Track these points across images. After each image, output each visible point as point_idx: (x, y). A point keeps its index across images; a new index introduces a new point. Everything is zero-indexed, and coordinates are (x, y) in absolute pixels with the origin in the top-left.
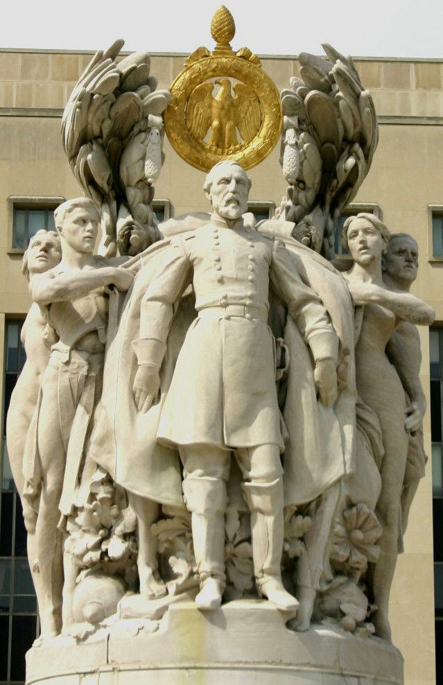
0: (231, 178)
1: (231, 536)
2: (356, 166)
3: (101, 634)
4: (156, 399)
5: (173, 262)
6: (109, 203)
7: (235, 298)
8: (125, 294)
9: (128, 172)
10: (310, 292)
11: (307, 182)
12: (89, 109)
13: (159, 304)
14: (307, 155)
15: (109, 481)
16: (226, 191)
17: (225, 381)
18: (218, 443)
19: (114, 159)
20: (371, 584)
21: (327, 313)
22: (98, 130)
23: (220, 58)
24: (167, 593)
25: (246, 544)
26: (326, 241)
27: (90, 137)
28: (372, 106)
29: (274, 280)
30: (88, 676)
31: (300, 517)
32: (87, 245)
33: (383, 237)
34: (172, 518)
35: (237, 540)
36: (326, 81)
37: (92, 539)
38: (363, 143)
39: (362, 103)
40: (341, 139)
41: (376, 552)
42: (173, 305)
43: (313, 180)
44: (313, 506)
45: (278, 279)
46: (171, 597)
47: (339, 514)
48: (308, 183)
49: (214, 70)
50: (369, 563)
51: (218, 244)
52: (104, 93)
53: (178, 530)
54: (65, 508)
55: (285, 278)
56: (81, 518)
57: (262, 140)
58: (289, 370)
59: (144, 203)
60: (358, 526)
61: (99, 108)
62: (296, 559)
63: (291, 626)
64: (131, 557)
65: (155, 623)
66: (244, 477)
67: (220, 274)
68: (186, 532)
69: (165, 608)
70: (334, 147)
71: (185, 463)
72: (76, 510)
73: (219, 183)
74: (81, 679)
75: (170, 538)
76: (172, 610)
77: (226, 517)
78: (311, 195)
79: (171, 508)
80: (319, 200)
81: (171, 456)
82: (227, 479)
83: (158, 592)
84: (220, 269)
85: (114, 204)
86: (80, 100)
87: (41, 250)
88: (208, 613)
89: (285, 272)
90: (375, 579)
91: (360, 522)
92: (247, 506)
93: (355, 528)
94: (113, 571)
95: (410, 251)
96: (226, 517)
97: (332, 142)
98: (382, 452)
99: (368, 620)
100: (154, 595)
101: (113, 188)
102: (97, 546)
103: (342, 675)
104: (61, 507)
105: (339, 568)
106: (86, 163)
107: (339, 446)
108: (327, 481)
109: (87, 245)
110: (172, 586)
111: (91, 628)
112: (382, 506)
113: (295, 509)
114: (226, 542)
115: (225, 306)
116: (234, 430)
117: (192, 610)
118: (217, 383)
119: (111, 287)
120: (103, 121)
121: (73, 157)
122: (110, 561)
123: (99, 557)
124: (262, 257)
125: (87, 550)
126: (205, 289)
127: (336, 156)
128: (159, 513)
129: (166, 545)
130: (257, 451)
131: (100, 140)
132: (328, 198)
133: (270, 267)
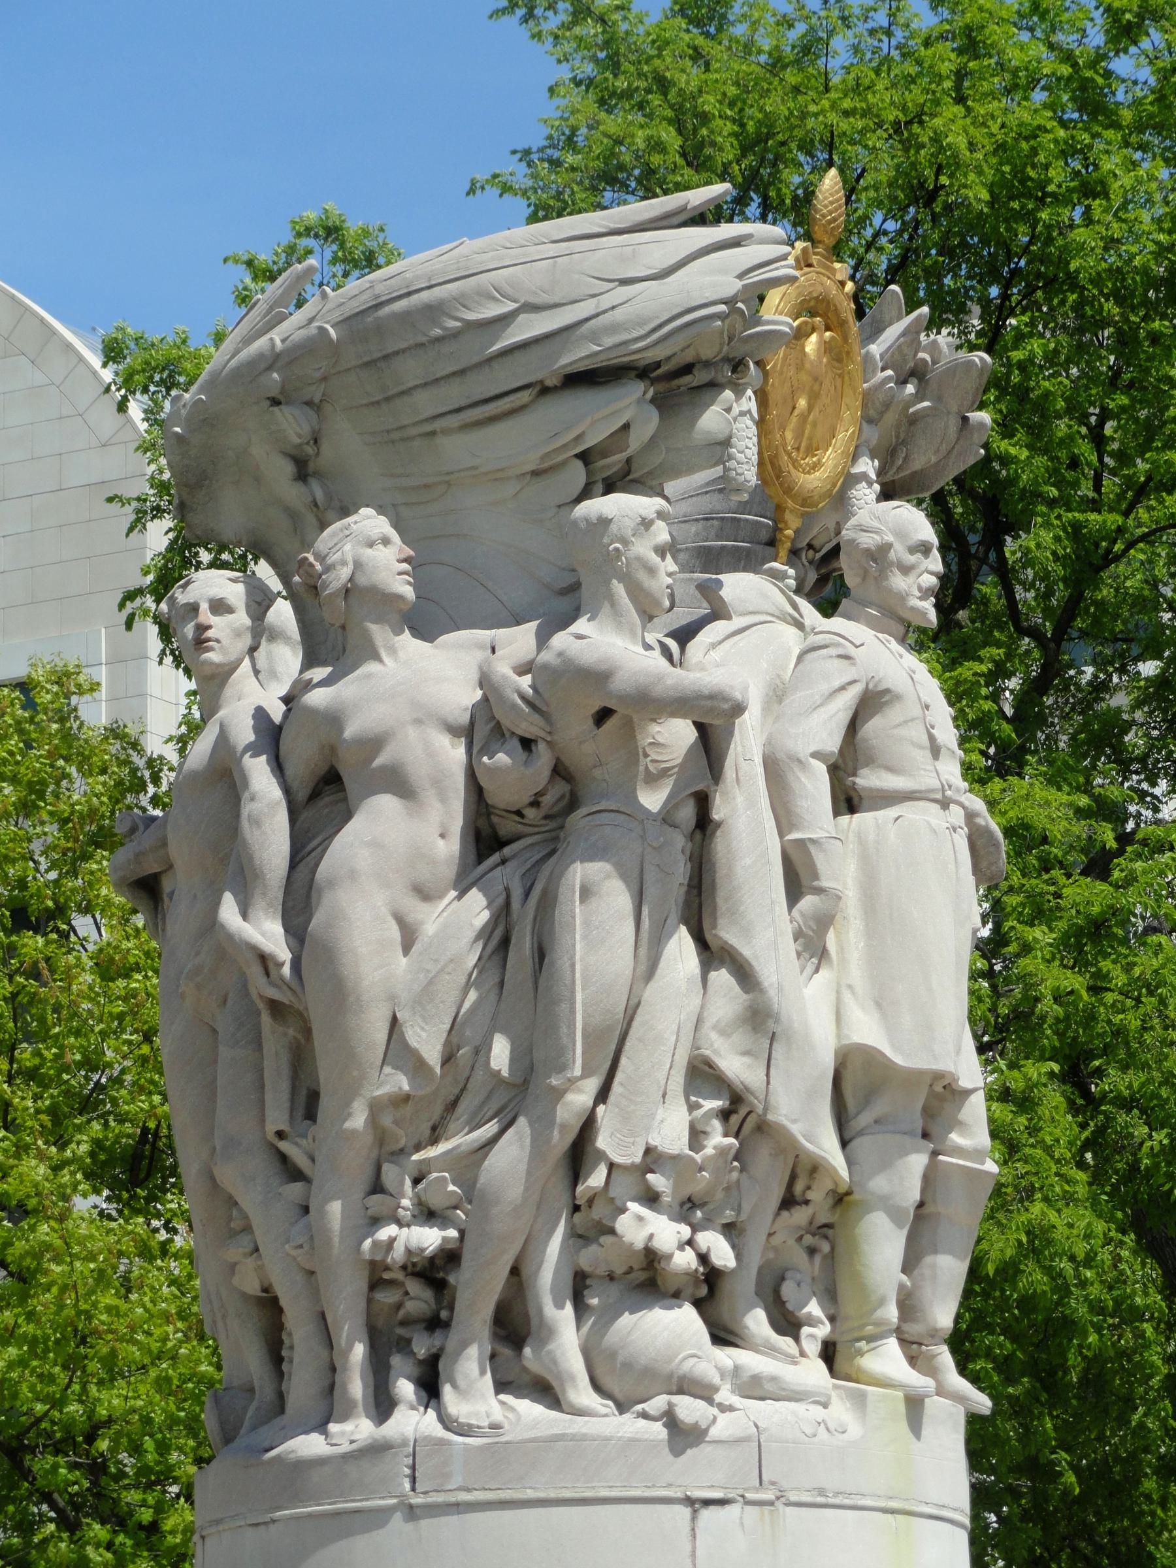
5: (843, 688)
30: (712, 1508)
34: (807, 1202)
72: (652, 1158)
73: (912, 550)
74: (695, 1511)
81: (856, 1088)
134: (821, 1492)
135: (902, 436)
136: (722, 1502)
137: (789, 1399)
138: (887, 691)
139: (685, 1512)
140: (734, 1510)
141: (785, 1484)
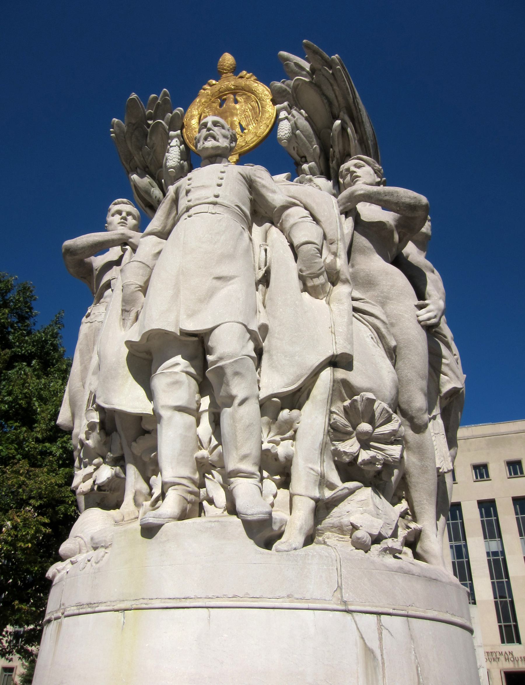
55: (264, 191)
89: (264, 186)
116: (192, 315)
130: (216, 331)
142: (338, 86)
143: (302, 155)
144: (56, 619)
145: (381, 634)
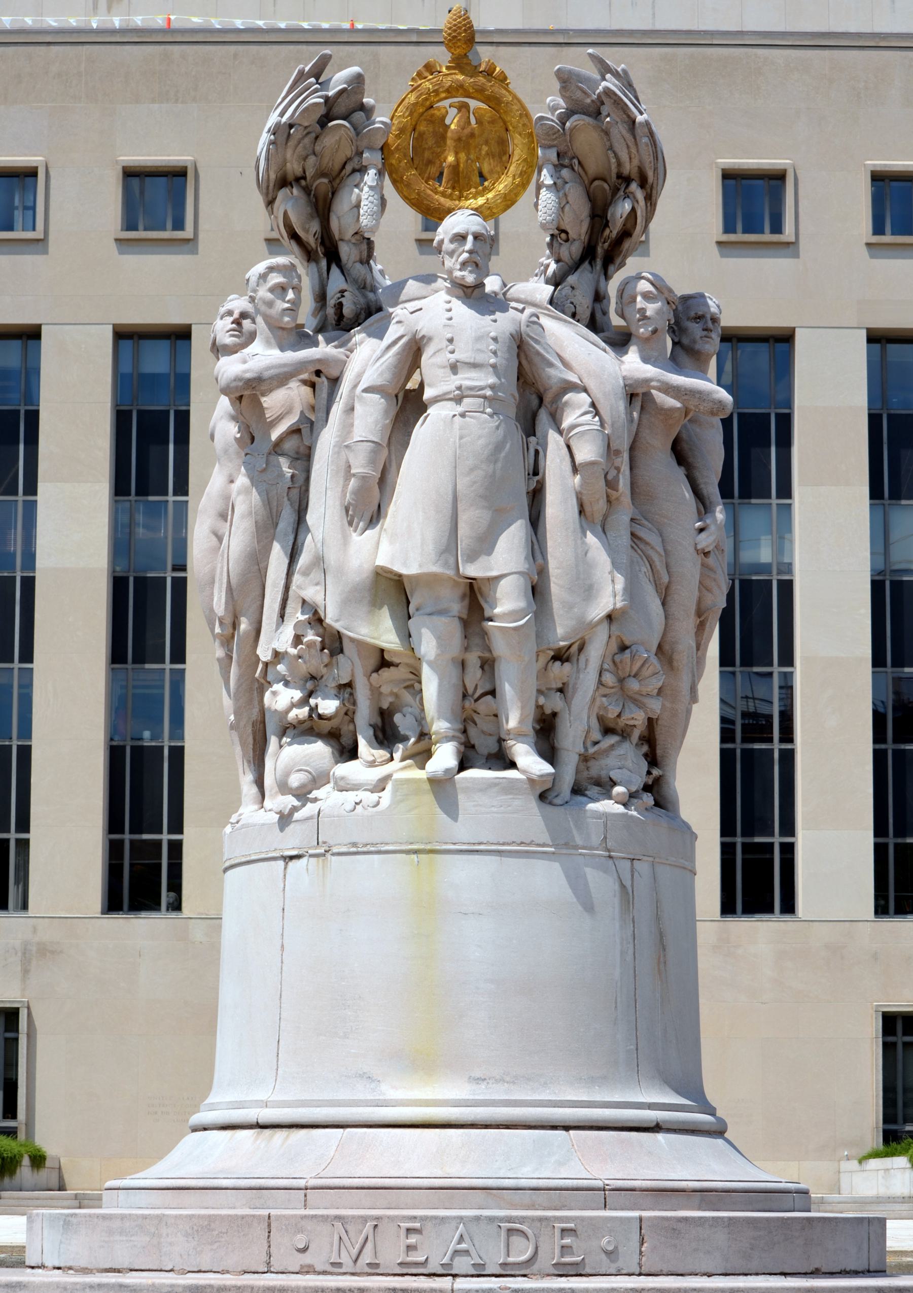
0: (467, 234)
1: (470, 691)
2: (633, 210)
3: (309, 809)
4: (375, 516)
6: (317, 261)
7: (471, 388)
8: (335, 382)
9: (339, 223)
10: (573, 378)
11: (569, 231)
12: (286, 143)
13: (376, 397)
14: (569, 198)
15: (317, 620)
16: (461, 249)
17: (459, 494)
18: (451, 573)
19: (322, 207)
20: (653, 748)
21: (593, 405)
22: (301, 169)
23: (455, 74)
24: (392, 759)
25: (489, 697)
26: (597, 306)
27: (290, 177)
28: (651, 134)
29: (524, 362)
31: (558, 663)
32: (286, 319)
33: (668, 303)
34: (397, 665)
35: (479, 692)
36: (593, 101)
37: (297, 695)
38: (643, 182)
39: (639, 131)
40: (614, 176)
41: (655, 706)
42: (396, 396)
43: (579, 229)
44: (575, 648)
45: (530, 362)
46: (396, 764)
47: (609, 660)
48: (572, 234)
49: (448, 91)
50: (650, 720)
51: (450, 319)
52: (306, 124)
53: (405, 680)
54: (264, 653)
55: (536, 360)
56: (281, 668)
57: (510, 179)
58: (544, 478)
59: (361, 262)
60: (633, 674)
61: (299, 143)
62: (554, 714)
63: (546, 798)
64: (348, 713)
65: (374, 797)
66: (487, 614)
67: (453, 358)
68: (414, 685)
69: (388, 778)
70: (606, 186)
71: (412, 596)
72: (278, 656)
75: (395, 690)
76: (396, 780)
77: (463, 664)
78: (576, 249)
79: (395, 653)
80: (588, 254)
81: (393, 591)
82: (465, 616)
83: (381, 757)
84: (452, 352)
85: (324, 263)
86: (274, 134)
87: (233, 323)
88: (440, 786)
90: (657, 737)
91: (635, 668)
92: (490, 651)
93: (629, 676)
94: (326, 731)
95: (708, 317)
96: (463, 664)
97: (605, 180)
98: (665, 579)
99: (647, 788)
100: (374, 761)
101: (323, 243)
102: (304, 701)
103: (610, 857)
104: (259, 652)
105: (612, 725)
106: (285, 213)
107: (607, 574)
108: (593, 615)
109: (286, 319)
110: (399, 750)
111: (296, 803)
112: (666, 647)
113: (552, 653)
114: (465, 696)
115: (458, 400)
116: (472, 558)
117: (420, 780)
118: (450, 498)
119: (318, 373)
120: (305, 159)
121: (270, 203)
122: (320, 717)
123: (306, 714)
124: (508, 334)
125: (293, 705)
126: (435, 379)
127: (610, 198)
128: (383, 661)
129: (391, 699)
130: (503, 582)
131: (303, 183)
132: (600, 251)
133: (519, 347)
134: (354, 844)
135: (608, 144)
136: (298, 857)
137: (353, 790)
138: (424, 337)
139: (281, 863)
140: (304, 861)
141: (331, 842)
142: (638, 151)
143: (563, 228)
144: (311, 856)
145: (632, 876)
